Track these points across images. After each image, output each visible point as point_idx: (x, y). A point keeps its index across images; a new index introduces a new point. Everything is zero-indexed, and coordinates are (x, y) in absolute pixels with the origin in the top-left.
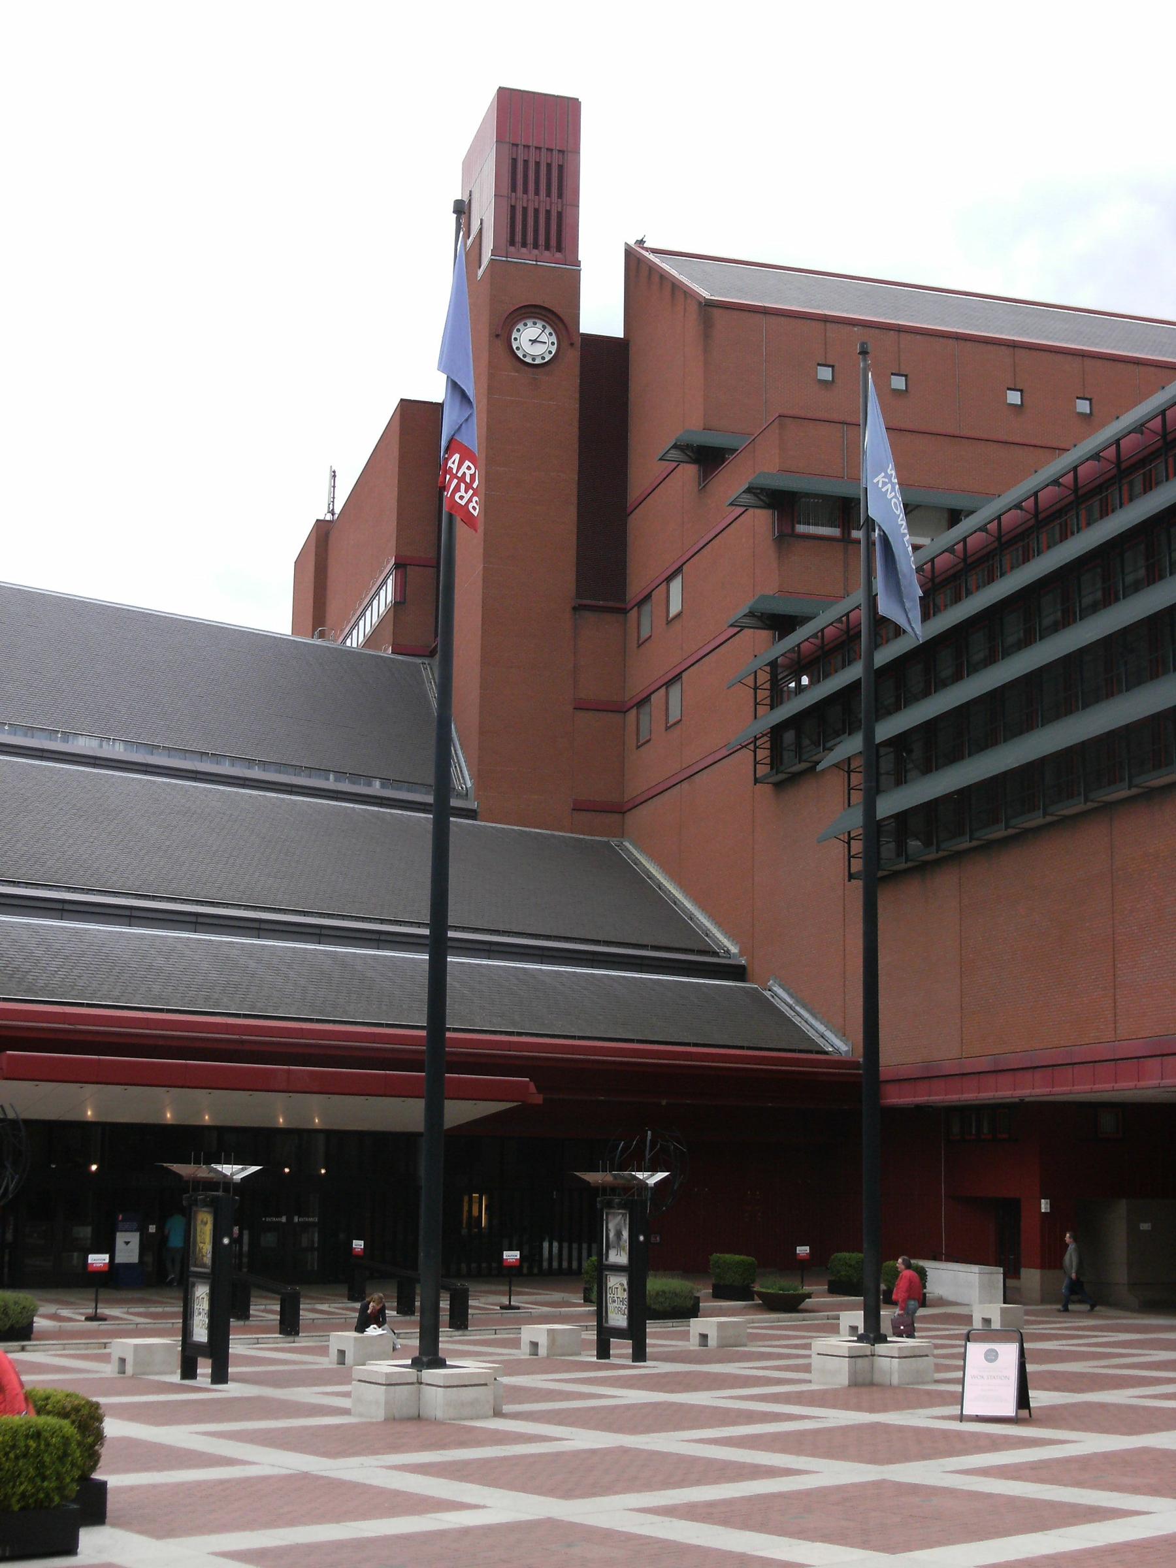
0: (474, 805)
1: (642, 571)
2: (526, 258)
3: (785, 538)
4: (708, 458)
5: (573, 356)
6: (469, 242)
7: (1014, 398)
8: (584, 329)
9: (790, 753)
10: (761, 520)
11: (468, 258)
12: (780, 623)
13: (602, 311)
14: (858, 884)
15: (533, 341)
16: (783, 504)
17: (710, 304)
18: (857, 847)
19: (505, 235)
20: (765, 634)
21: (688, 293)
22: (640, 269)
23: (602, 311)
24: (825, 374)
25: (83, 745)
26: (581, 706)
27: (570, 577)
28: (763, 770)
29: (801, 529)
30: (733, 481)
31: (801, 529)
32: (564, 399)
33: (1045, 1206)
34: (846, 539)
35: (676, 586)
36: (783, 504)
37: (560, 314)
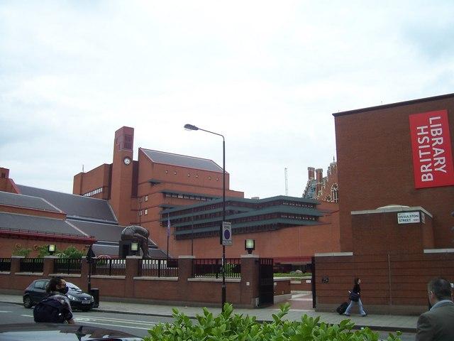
1: (140, 194)
3: (165, 197)
4: (153, 183)
9: (164, 224)
12: (164, 208)
13: (135, 158)
15: (127, 161)
16: (164, 193)
23: (135, 158)
25: (74, 217)
26: (132, 210)
30: (156, 188)
32: (131, 168)
36: (164, 193)
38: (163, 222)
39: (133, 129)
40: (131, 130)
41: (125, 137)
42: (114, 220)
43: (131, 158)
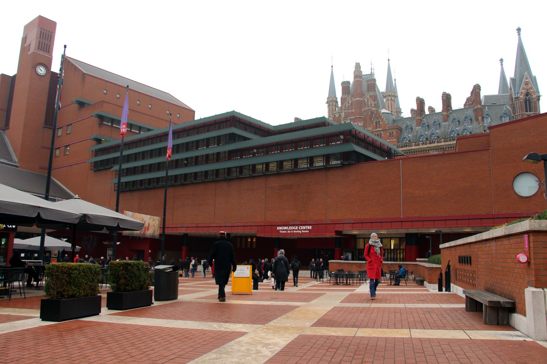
0: (18, 165)
2: (41, 53)
3: (101, 124)
4: (81, 105)
5: (49, 75)
6: (26, 45)
7: (138, 102)
8: (52, 70)
10: (96, 120)
11: (24, 49)
12: (99, 141)
13: (56, 67)
14: (116, 192)
15: (41, 71)
16: (101, 118)
17: (85, 74)
18: (116, 185)
19: (37, 47)
20: (95, 142)
21: (79, 70)
22: (65, 60)
23: (56, 67)
24: (105, 92)
27: (43, 121)
28: (92, 168)
29: (104, 123)
31: (104, 123)
32: (46, 84)
33: (150, 251)
34: (112, 126)
35: (70, 127)
37: (47, 66)
38: (96, 163)
39: (53, 25)
40: (53, 25)
41: (42, 33)
42: (11, 160)
43: (48, 67)
